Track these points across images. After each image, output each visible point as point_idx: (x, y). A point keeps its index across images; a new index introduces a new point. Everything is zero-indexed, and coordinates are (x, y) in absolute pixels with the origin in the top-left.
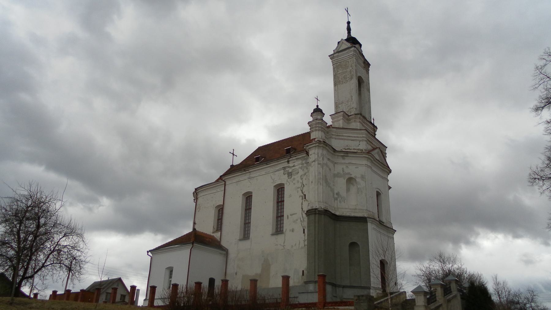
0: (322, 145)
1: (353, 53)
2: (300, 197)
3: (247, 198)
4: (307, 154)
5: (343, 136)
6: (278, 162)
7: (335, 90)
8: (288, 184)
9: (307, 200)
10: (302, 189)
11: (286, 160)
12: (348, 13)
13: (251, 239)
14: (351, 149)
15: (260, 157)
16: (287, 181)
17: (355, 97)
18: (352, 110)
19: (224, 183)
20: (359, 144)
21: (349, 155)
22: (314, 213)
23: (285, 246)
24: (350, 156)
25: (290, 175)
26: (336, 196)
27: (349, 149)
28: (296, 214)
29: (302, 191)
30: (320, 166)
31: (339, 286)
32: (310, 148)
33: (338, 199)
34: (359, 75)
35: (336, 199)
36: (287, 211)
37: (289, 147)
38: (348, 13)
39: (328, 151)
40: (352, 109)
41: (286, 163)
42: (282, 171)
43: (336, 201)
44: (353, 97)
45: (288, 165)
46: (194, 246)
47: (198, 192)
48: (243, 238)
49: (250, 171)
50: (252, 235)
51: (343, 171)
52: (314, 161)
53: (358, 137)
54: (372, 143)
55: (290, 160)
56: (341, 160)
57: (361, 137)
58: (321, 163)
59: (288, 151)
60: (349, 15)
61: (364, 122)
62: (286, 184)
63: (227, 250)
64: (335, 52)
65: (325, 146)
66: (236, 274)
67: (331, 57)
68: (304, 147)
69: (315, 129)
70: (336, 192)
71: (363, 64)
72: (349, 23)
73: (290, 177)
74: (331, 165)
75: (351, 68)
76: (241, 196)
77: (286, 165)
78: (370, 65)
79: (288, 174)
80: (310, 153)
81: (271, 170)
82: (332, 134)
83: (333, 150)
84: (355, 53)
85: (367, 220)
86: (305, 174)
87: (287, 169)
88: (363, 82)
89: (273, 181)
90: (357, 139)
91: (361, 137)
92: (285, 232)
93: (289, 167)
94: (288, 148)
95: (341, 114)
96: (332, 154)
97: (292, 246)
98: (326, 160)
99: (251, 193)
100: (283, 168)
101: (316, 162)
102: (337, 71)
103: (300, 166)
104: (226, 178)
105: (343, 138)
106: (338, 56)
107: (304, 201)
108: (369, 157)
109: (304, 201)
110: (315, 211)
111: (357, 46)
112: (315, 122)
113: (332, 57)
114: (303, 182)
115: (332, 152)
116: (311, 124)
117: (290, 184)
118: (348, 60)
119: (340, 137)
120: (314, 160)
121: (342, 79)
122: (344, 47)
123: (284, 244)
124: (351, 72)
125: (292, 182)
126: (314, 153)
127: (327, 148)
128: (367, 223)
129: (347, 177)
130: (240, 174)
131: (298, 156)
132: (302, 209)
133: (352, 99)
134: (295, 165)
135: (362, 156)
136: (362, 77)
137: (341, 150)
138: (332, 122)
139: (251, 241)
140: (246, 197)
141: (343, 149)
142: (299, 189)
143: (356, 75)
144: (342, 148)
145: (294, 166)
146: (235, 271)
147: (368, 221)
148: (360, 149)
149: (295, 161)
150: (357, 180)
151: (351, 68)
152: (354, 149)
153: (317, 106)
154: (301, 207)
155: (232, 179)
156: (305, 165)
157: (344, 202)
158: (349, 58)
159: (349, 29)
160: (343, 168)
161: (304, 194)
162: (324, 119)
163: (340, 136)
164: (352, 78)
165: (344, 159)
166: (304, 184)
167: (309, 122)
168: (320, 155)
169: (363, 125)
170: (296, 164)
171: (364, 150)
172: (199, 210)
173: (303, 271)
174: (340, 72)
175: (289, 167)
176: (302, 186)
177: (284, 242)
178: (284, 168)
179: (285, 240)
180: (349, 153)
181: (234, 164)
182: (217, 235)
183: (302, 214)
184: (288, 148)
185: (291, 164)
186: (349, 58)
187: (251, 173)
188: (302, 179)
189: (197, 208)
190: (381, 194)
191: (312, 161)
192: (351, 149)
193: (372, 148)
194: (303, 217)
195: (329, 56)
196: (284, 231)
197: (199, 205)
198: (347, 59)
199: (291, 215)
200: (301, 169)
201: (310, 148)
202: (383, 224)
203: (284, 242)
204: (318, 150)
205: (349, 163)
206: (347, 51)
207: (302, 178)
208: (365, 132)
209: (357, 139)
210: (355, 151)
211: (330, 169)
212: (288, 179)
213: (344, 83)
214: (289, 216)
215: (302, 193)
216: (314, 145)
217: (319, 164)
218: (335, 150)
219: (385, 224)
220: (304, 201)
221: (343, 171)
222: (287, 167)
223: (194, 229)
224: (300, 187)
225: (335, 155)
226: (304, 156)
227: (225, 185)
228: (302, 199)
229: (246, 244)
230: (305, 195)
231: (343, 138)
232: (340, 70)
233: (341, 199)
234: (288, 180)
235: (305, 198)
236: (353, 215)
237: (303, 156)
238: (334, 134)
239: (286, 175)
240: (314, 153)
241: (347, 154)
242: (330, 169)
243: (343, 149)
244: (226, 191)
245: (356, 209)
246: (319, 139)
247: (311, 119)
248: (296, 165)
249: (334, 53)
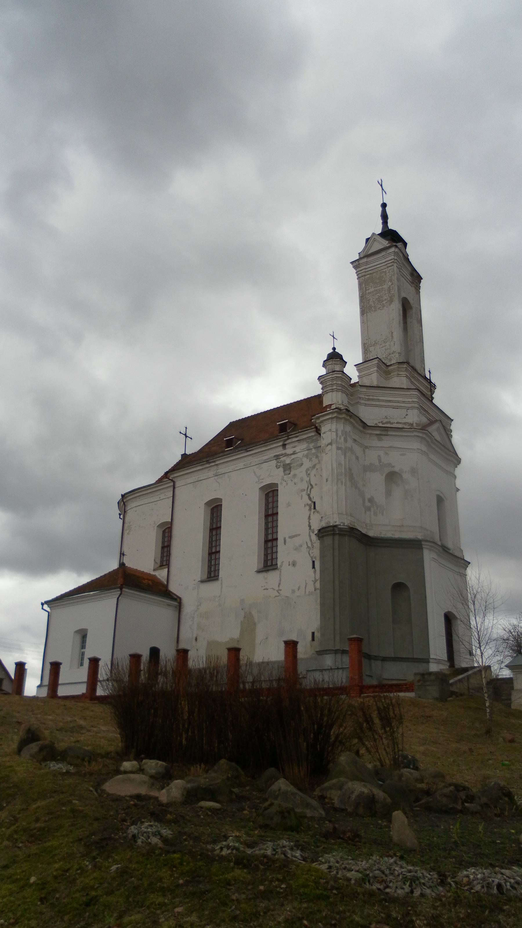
0: (344, 416)
1: (393, 257)
2: (305, 506)
3: (212, 509)
4: (318, 431)
5: (378, 400)
6: (266, 446)
7: (363, 323)
8: (284, 483)
9: (318, 512)
10: (309, 492)
11: (281, 444)
12: (383, 189)
13: (222, 580)
14: (392, 423)
15: (234, 440)
16: (283, 479)
17: (398, 333)
18: (392, 355)
19: (172, 484)
20: (407, 415)
21: (389, 433)
22: (332, 532)
23: (281, 590)
24: (391, 435)
25: (287, 468)
26: (368, 504)
27: (389, 422)
28: (299, 535)
29: (309, 495)
30: (340, 451)
31: (376, 658)
32: (322, 422)
33: (372, 509)
34: (404, 295)
35: (368, 509)
36: (282, 532)
37: (286, 420)
38: (383, 189)
40: (392, 353)
41: (281, 448)
42: (274, 462)
43: (368, 513)
44: (395, 334)
45: (284, 452)
46: (123, 593)
47: (126, 501)
48: (208, 578)
49: (217, 463)
50: (222, 574)
51: (380, 461)
52: (331, 444)
53: (404, 402)
54: (429, 413)
55: (288, 443)
56: (375, 442)
57: (409, 402)
58: (343, 446)
59: (283, 428)
60: (384, 193)
61: (414, 377)
62: (281, 483)
63: (180, 598)
64: (362, 256)
65: (349, 418)
66: (196, 639)
67: (355, 264)
68: (311, 420)
69: (330, 388)
70: (368, 496)
71: (409, 277)
72: (384, 205)
73: (288, 472)
74: (358, 450)
75: (390, 284)
76: (203, 506)
77: (280, 451)
78: (422, 279)
79: (284, 468)
80: (323, 429)
81: (256, 460)
82: (360, 398)
83: (361, 424)
84: (396, 258)
85: (421, 545)
86: (314, 467)
87: (281, 459)
88: (411, 308)
89: (257, 480)
90: (403, 405)
91: (409, 402)
92: (281, 566)
93: (286, 455)
94: (283, 422)
95: (374, 363)
96: (361, 431)
97: (293, 591)
98: (350, 443)
99: (220, 500)
100: (275, 456)
101: (334, 446)
102: (366, 288)
103: (305, 453)
104: (176, 475)
105: (378, 403)
106: (367, 263)
107: (312, 513)
108: (424, 436)
109: (314, 512)
110: (333, 530)
111: (400, 245)
112: (331, 376)
113: (356, 264)
114: (310, 480)
115: (361, 429)
116: (323, 379)
117: (287, 484)
118: (384, 270)
119: (374, 403)
120: (330, 441)
121: (374, 303)
122: (377, 246)
123: (279, 586)
124: (389, 290)
125: (292, 481)
126: (330, 430)
127: (352, 420)
128: (422, 549)
129: (387, 470)
130: (201, 468)
131: (302, 435)
132: (310, 526)
133: (392, 337)
134: (295, 451)
135: (413, 435)
136: (408, 298)
137: (376, 424)
138: (358, 376)
139: (222, 584)
140: (212, 507)
141: (379, 423)
142: (304, 493)
143: (399, 296)
144: (376, 422)
145: (294, 453)
146: (195, 636)
147: (423, 546)
148: (408, 423)
149: (296, 444)
150: (405, 476)
151: (390, 284)
152: (398, 423)
153: (334, 349)
154: (308, 523)
155: (186, 476)
156: (314, 451)
157: (383, 514)
158: (386, 267)
159: (385, 217)
160: (379, 456)
161: (312, 502)
162: (346, 370)
163: (373, 400)
164: (391, 301)
165: (380, 440)
166: (312, 483)
167: (320, 377)
168: (340, 433)
169: (412, 382)
170: (297, 449)
171: (415, 425)
172: (130, 531)
173: (313, 634)
174: (372, 290)
175: (286, 455)
176: (310, 487)
177: (279, 584)
178: (277, 457)
179: (280, 580)
180: (389, 429)
181: (188, 452)
182: (162, 575)
183: (310, 536)
184: (283, 422)
185: (289, 451)
186: (386, 267)
187: (220, 466)
188: (308, 475)
189: (126, 528)
190: (444, 500)
191: (327, 444)
192: (392, 423)
193: (428, 422)
194: (311, 540)
195: (352, 263)
196: (279, 564)
197: (130, 523)
198: (382, 268)
199: (291, 537)
200: (307, 458)
201: (322, 422)
202: (448, 551)
203: (279, 584)
204: (336, 425)
205: (390, 447)
206: (383, 253)
207: (309, 474)
208: (416, 393)
209: (403, 405)
210: (400, 426)
211: (357, 458)
212: (285, 475)
213: (378, 309)
214: (287, 539)
215: (310, 499)
216: (330, 416)
217: (338, 448)
218: (364, 425)
219: (451, 552)
220: (312, 513)
221: (380, 461)
222: (282, 455)
223: (122, 565)
224: (306, 489)
225: (365, 433)
226: (312, 436)
227: (174, 488)
228: (310, 510)
229: (212, 588)
230: (314, 503)
231: (378, 403)
232: (371, 287)
233: (377, 509)
234: (285, 477)
235: (315, 508)
236: (397, 535)
237: (310, 435)
238: (363, 396)
239: (281, 469)
240: (330, 430)
241: (387, 431)
242: (357, 458)
243: (379, 423)
244: (177, 498)
245: (403, 526)
246: (338, 406)
247: (323, 371)
248: (297, 451)
249: (360, 258)
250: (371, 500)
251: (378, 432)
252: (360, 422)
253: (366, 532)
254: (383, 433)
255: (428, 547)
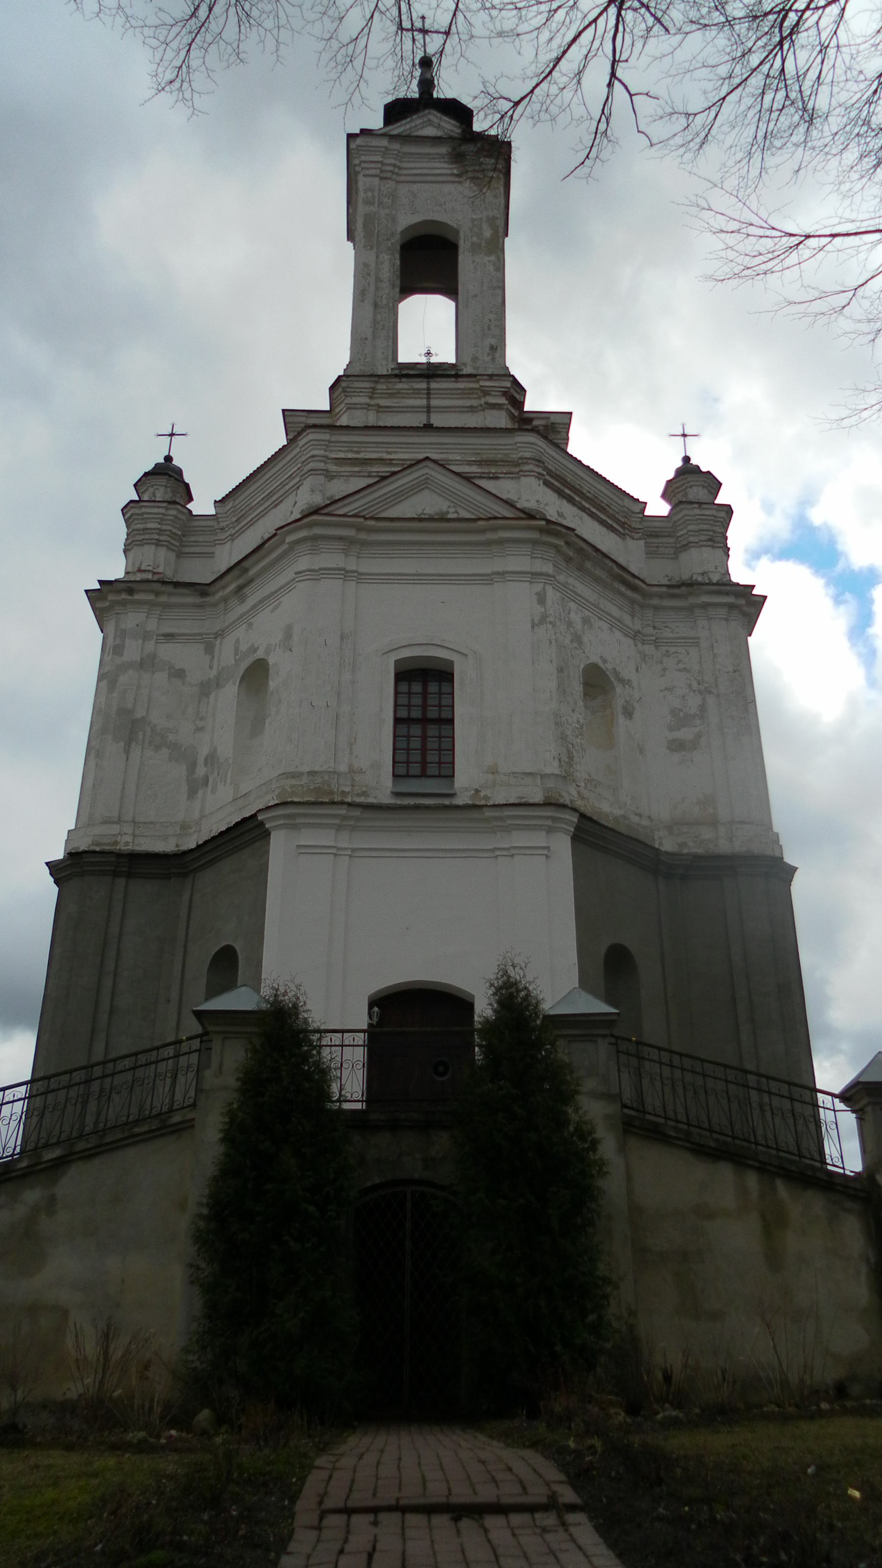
21: (251, 573)
39: (152, 604)
65: (124, 596)
115: (198, 600)
128: (267, 834)
135: (285, 547)
165: (242, 600)
202: (447, 802)
211: (179, 674)
241: (246, 570)
250: (211, 759)
251: (232, 587)
252: (170, 589)
253: (177, 846)
254: (241, 581)
255: (281, 822)
